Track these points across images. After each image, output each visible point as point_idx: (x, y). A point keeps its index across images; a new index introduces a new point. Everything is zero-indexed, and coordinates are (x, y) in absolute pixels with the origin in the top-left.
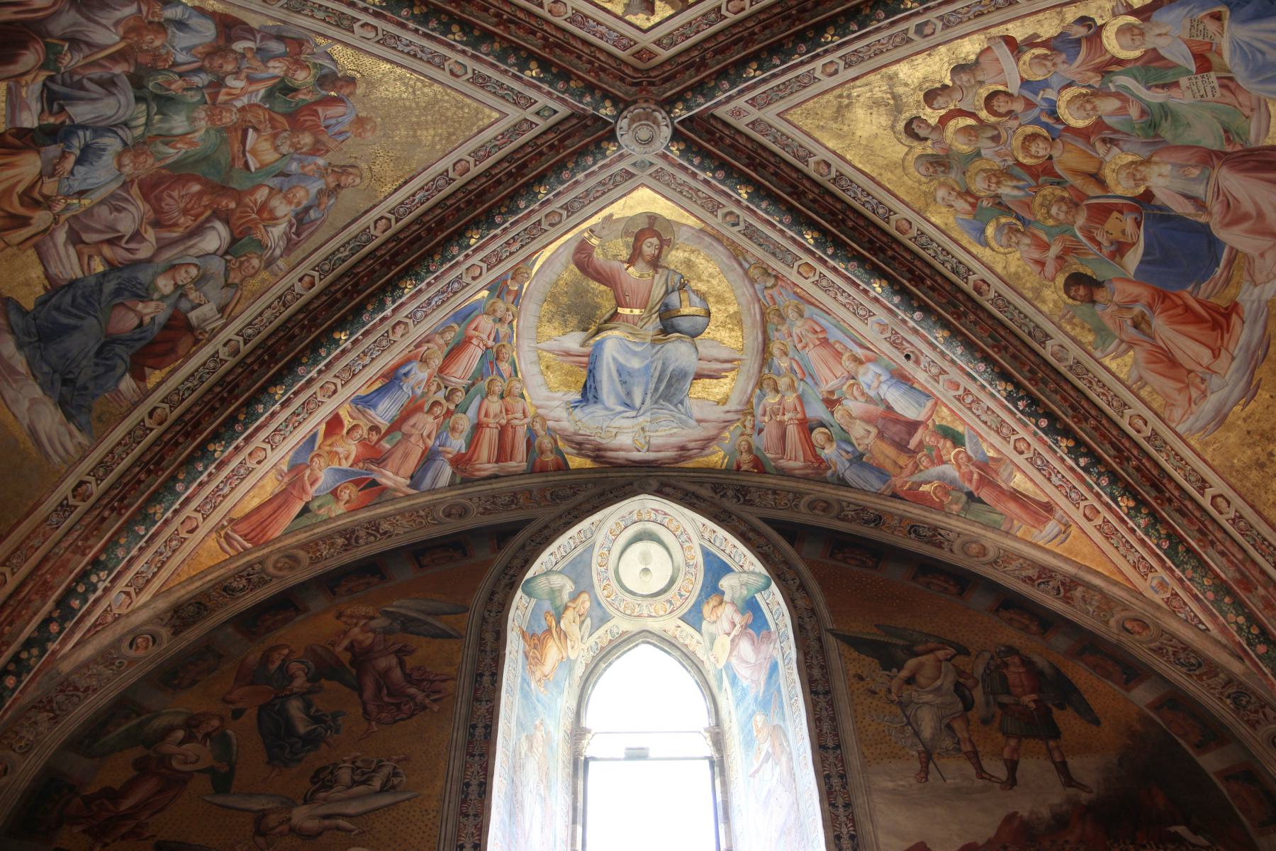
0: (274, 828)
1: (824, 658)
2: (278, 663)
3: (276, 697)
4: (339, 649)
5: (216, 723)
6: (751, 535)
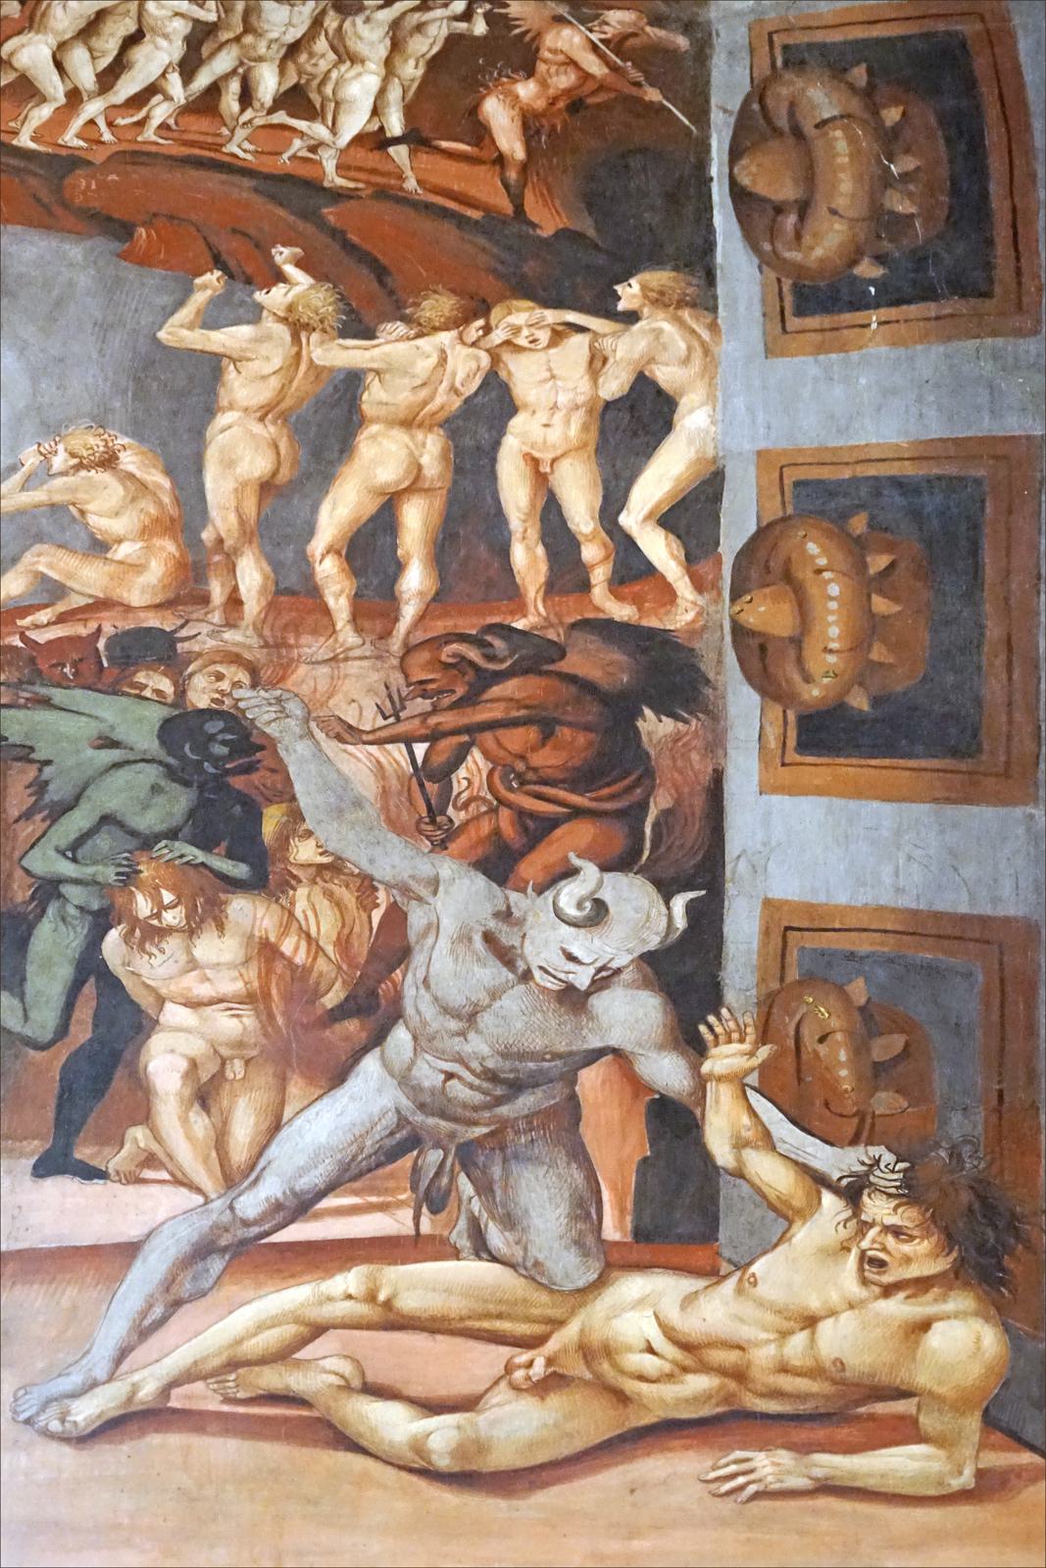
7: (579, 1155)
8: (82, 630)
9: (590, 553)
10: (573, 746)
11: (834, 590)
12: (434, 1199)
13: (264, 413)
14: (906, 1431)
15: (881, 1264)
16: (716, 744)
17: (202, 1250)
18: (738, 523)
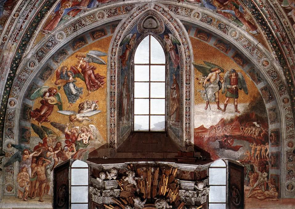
0: (73, 119)
2: (65, 73)
3: (67, 83)
4: (78, 68)
5: (55, 90)
6: (177, 27)
10: (264, 167)
14: (274, 198)
16: (269, 166)
18: (270, 156)
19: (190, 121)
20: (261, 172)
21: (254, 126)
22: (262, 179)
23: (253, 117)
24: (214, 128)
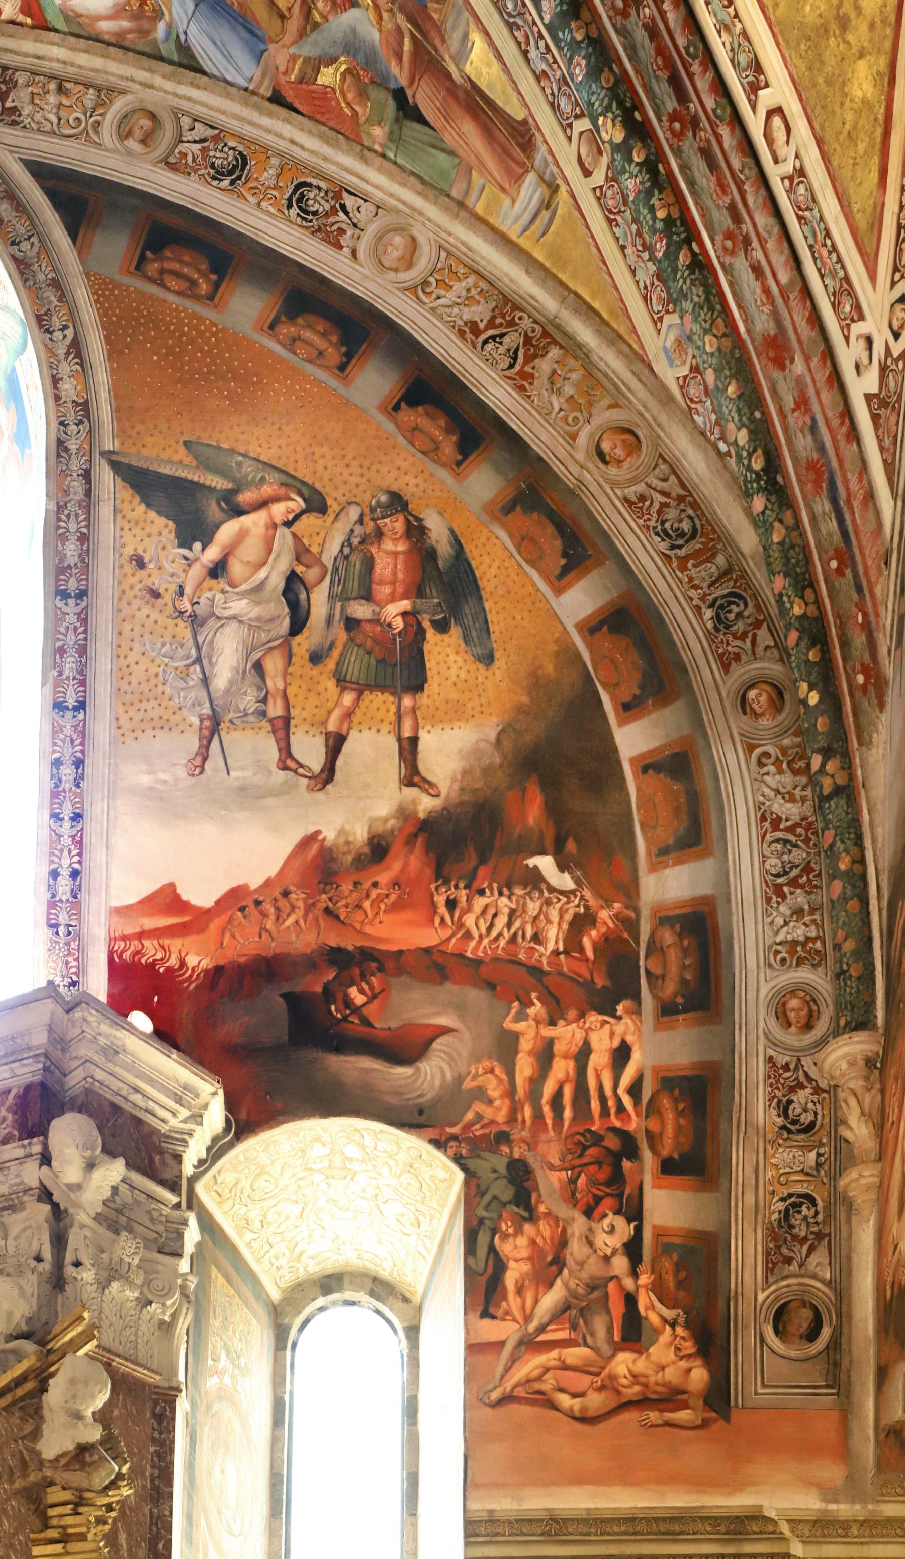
1: (88, 519)
7: (608, 1312)
8: (487, 1131)
9: (611, 1103)
11: (670, 1116)
12: (574, 1327)
13: (530, 1053)
14: (685, 1406)
15: (679, 1349)
16: (641, 1171)
17: (520, 1343)
18: (647, 1093)
19: (80, 855)
20: (588, 1213)
21: (535, 879)
22: (593, 1260)
23: (531, 821)
24: (249, 902)
